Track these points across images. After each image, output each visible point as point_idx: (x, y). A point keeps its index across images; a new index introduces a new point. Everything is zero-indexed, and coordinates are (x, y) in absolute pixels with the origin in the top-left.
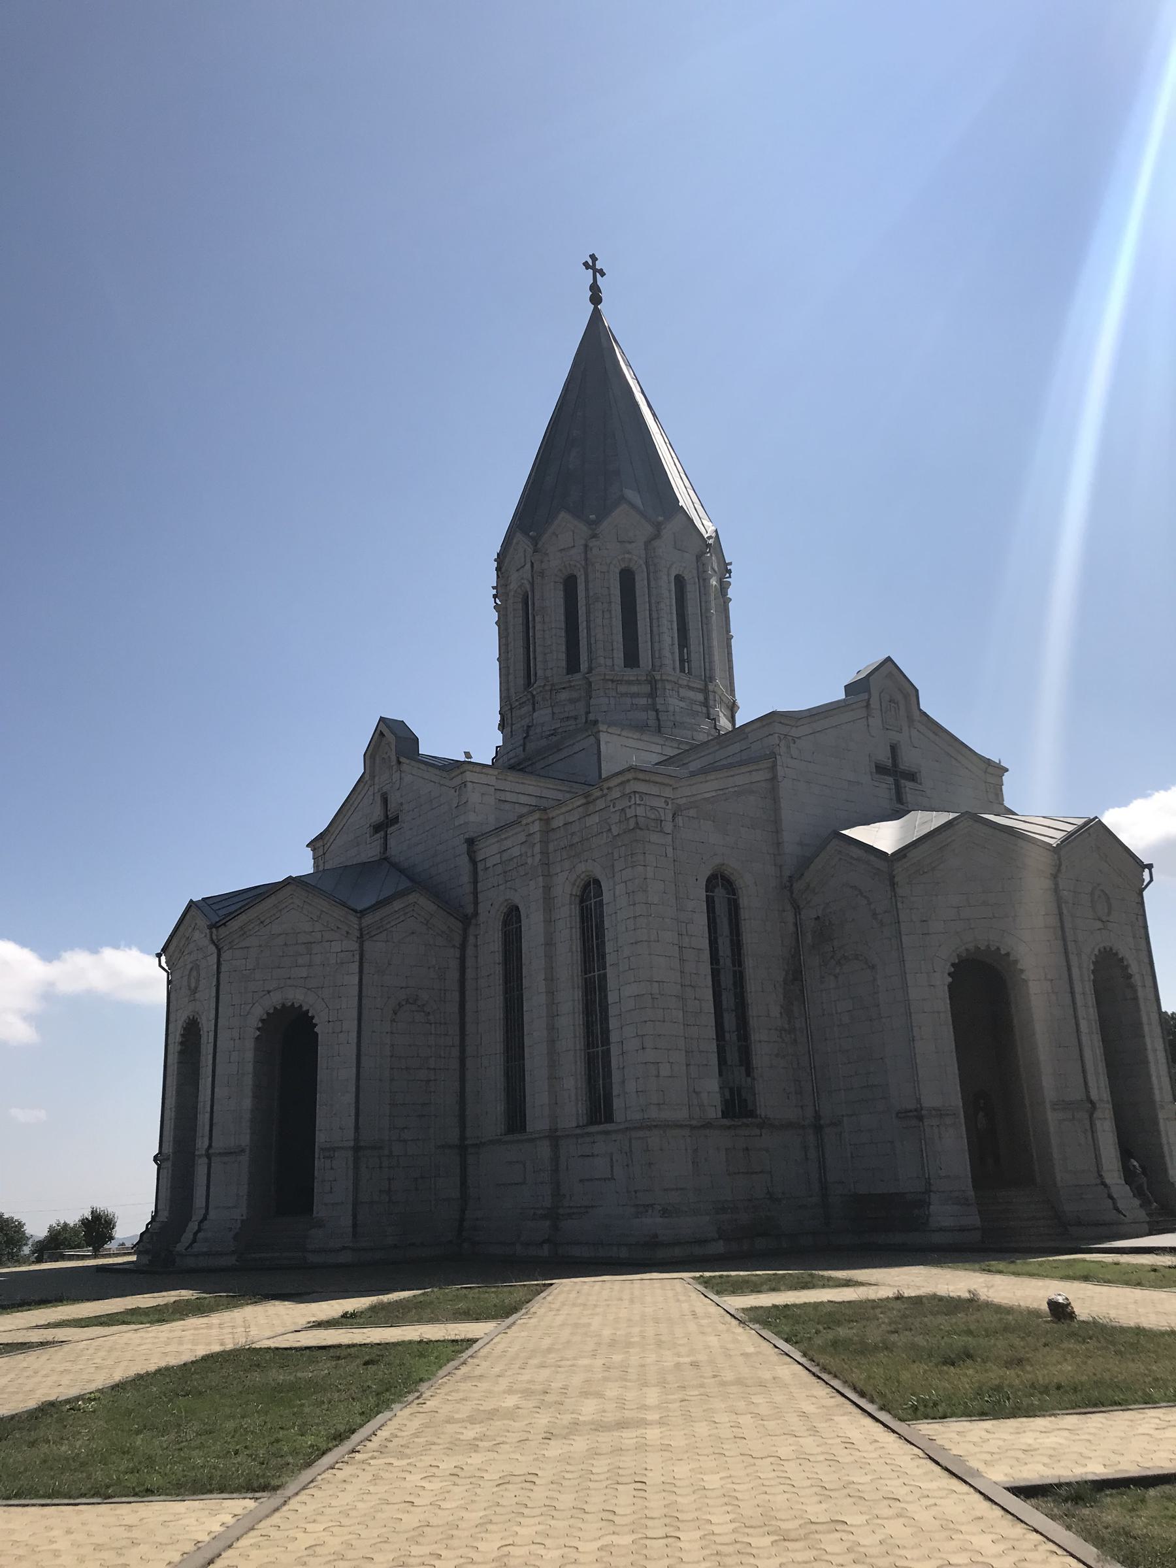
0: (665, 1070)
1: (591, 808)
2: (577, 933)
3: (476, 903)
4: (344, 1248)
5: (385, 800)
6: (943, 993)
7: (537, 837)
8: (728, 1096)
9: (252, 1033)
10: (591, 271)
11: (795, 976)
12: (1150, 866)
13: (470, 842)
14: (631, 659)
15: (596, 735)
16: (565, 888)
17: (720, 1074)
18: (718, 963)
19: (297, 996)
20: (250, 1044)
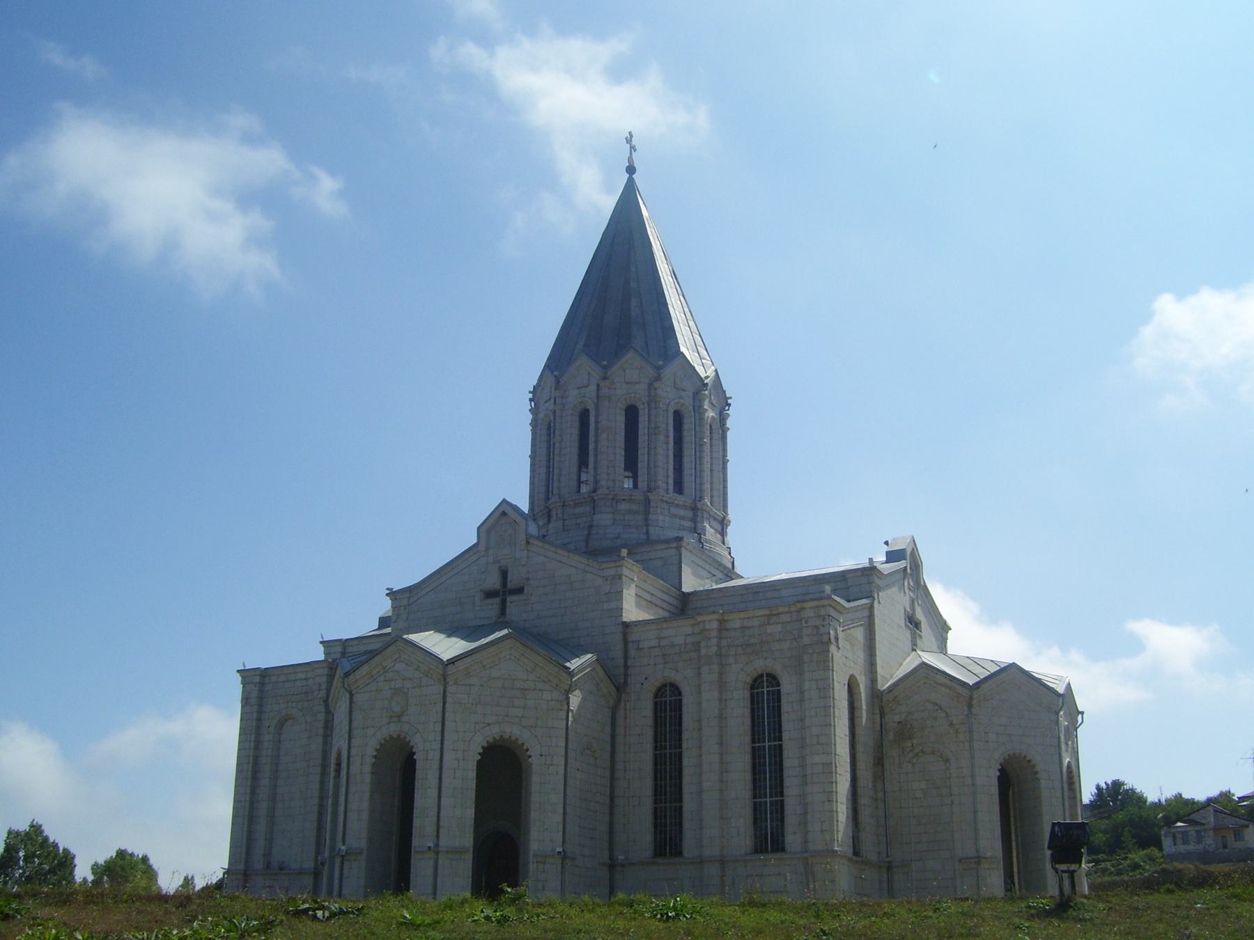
1: (774, 619)
2: (747, 712)
3: (626, 675)
5: (504, 574)
7: (715, 633)
11: (879, 762)
12: (1082, 713)
13: (626, 625)
14: (679, 487)
15: (679, 549)
16: (740, 674)
19: (513, 731)
20: (472, 765)
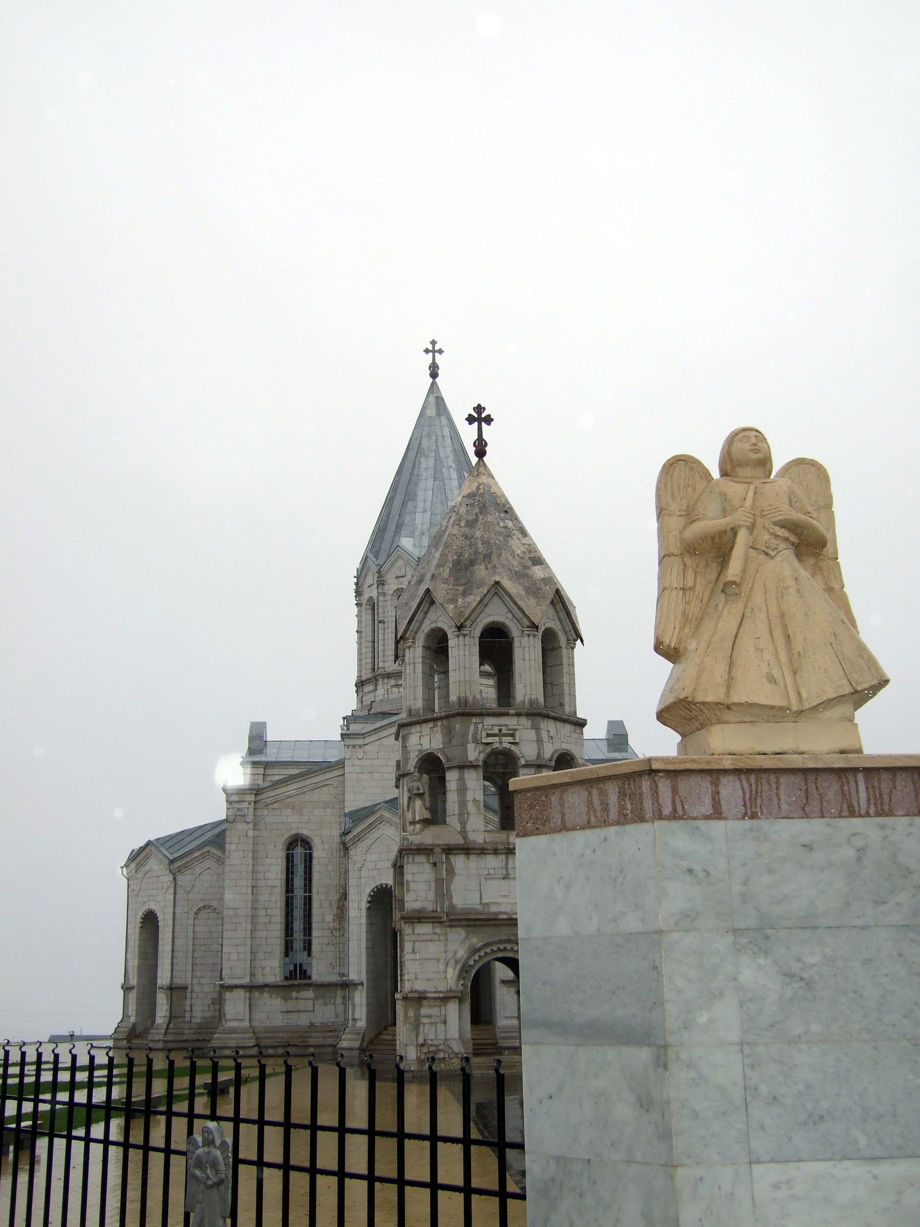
0: (234, 956)
4: (159, 1040)
6: (364, 913)
8: (292, 968)
9: (138, 925)
10: (431, 354)
17: (287, 955)
18: (292, 892)
19: (153, 906)
